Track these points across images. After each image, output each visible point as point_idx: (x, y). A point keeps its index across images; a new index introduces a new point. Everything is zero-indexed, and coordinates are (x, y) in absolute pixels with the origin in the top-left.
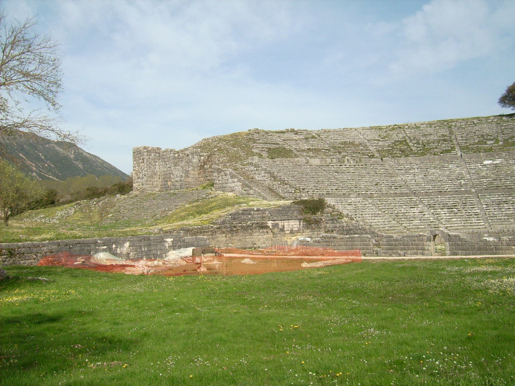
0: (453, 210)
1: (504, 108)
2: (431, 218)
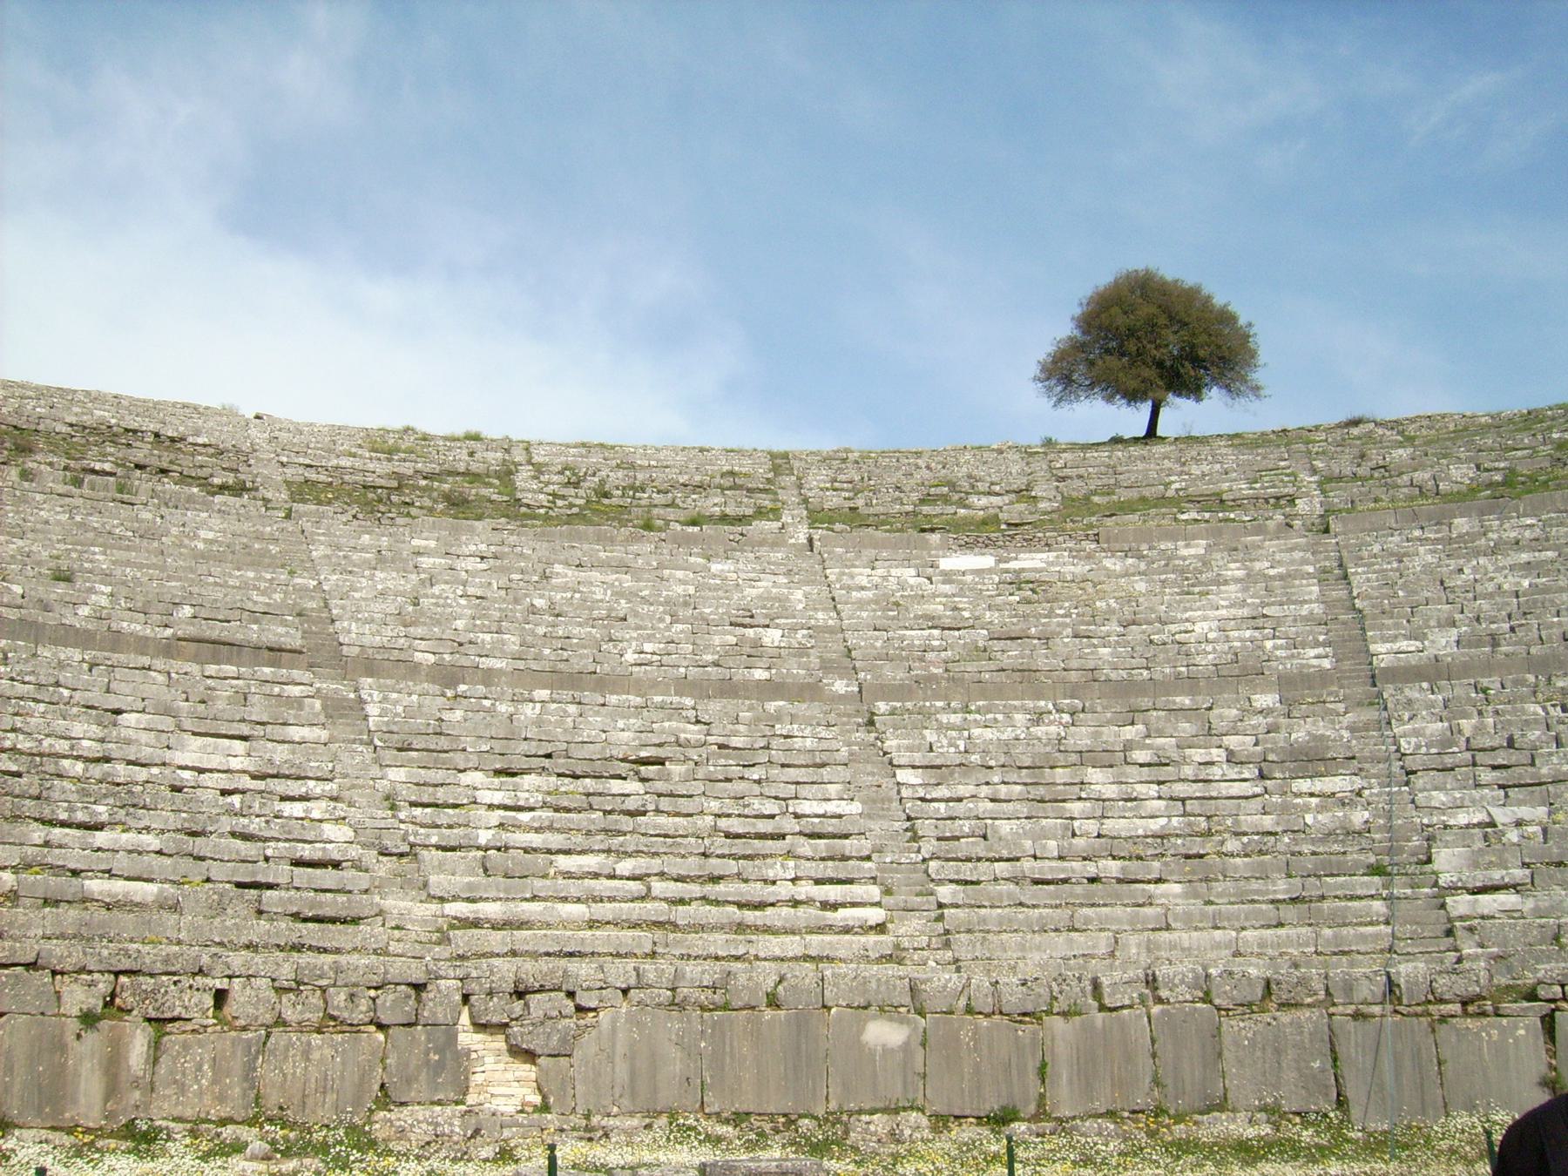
0: (616, 786)
1: (1066, 407)
2: (329, 830)
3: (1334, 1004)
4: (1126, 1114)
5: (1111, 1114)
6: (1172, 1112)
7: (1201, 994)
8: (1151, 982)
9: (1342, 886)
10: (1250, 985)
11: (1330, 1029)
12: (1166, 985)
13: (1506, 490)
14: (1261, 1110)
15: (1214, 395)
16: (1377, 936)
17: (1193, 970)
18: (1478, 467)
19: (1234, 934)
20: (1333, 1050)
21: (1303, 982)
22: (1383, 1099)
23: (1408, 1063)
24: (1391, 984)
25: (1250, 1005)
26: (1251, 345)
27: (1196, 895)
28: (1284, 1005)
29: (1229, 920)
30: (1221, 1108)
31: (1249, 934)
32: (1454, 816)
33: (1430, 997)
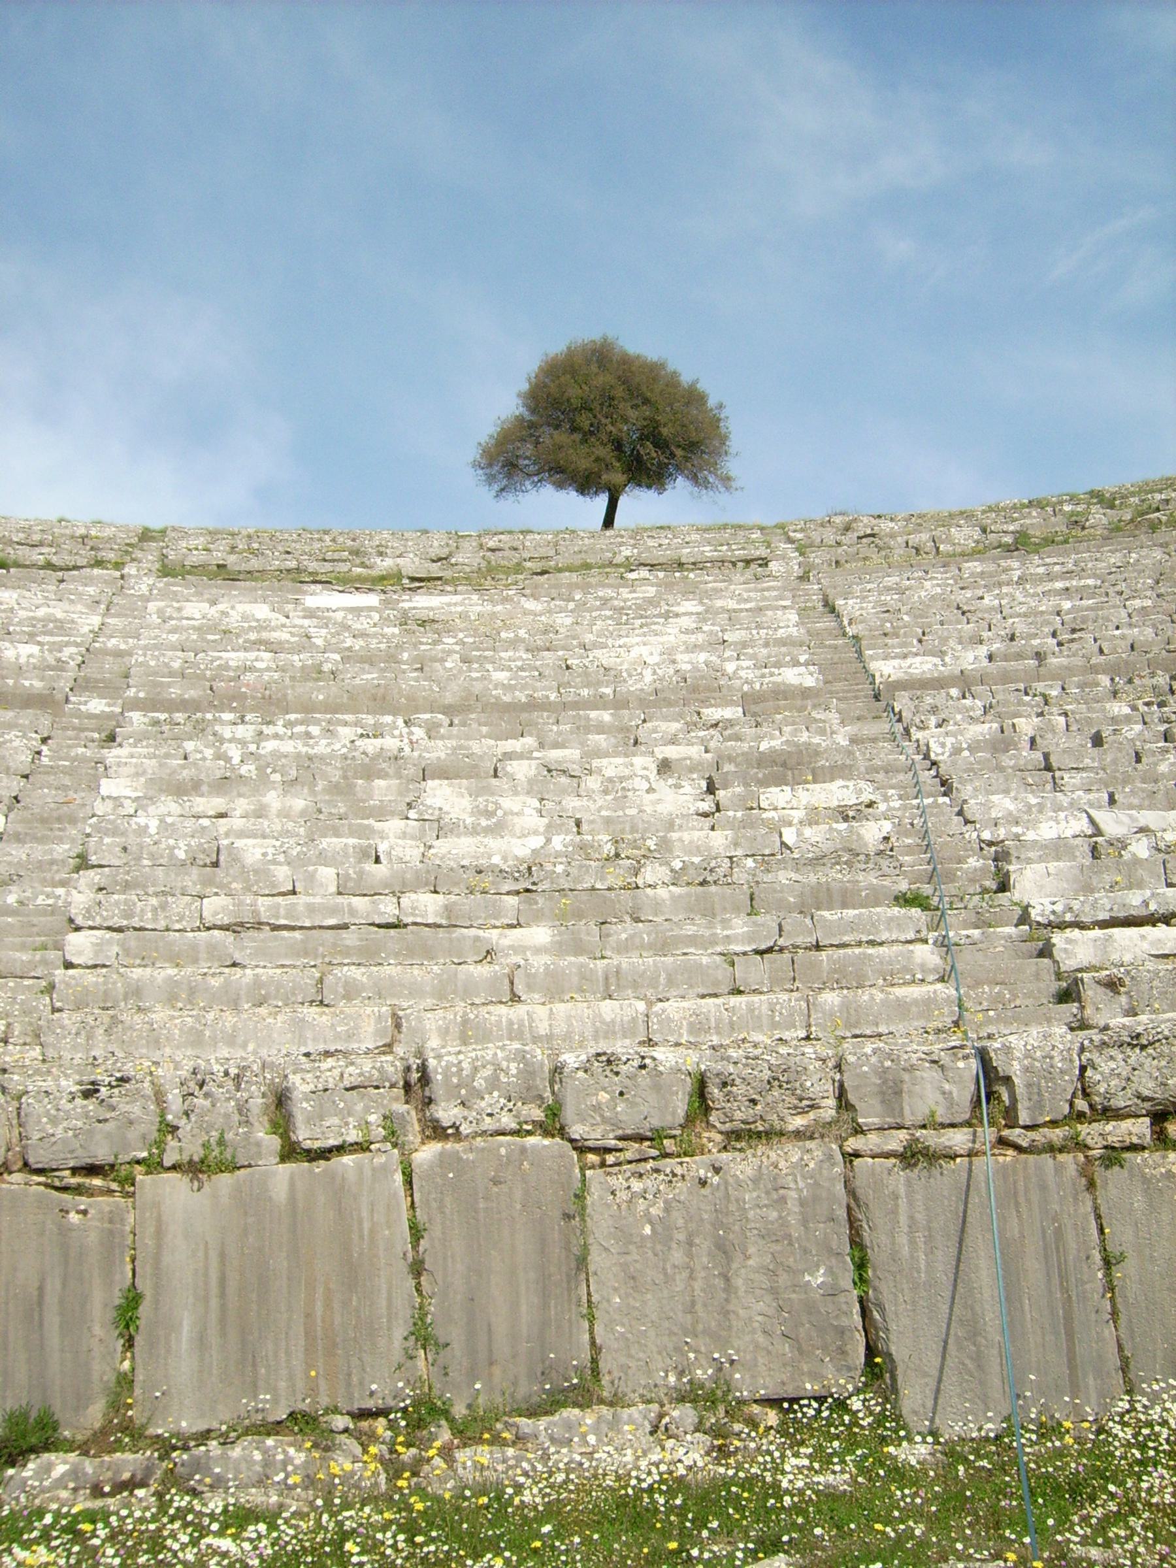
1: (510, 497)
3: (858, 1131)
4: (341, 1422)
5: (302, 1423)
6: (459, 1410)
7: (538, 1114)
8: (417, 1085)
9: (852, 926)
10: (657, 1087)
11: (852, 1192)
12: (452, 1091)
13: (1021, 544)
14: (682, 1399)
15: (680, 486)
16: (928, 1004)
17: (521, 1056)
18: (984, 531)
19: (641, 1006)
20: (856, 1241)
21: (783, 1078)
22: (978, 1358)
23: (1033, 1266)
24: (991, 1077)
25: (655, 1137)
26: (723, 431)
27: (578, 948)
28: (736, 1137)
29: (635, 985)
30: (584, 1395)
31: (675, 1008)
32: (1033, 824)
33: (1081, 1105)
